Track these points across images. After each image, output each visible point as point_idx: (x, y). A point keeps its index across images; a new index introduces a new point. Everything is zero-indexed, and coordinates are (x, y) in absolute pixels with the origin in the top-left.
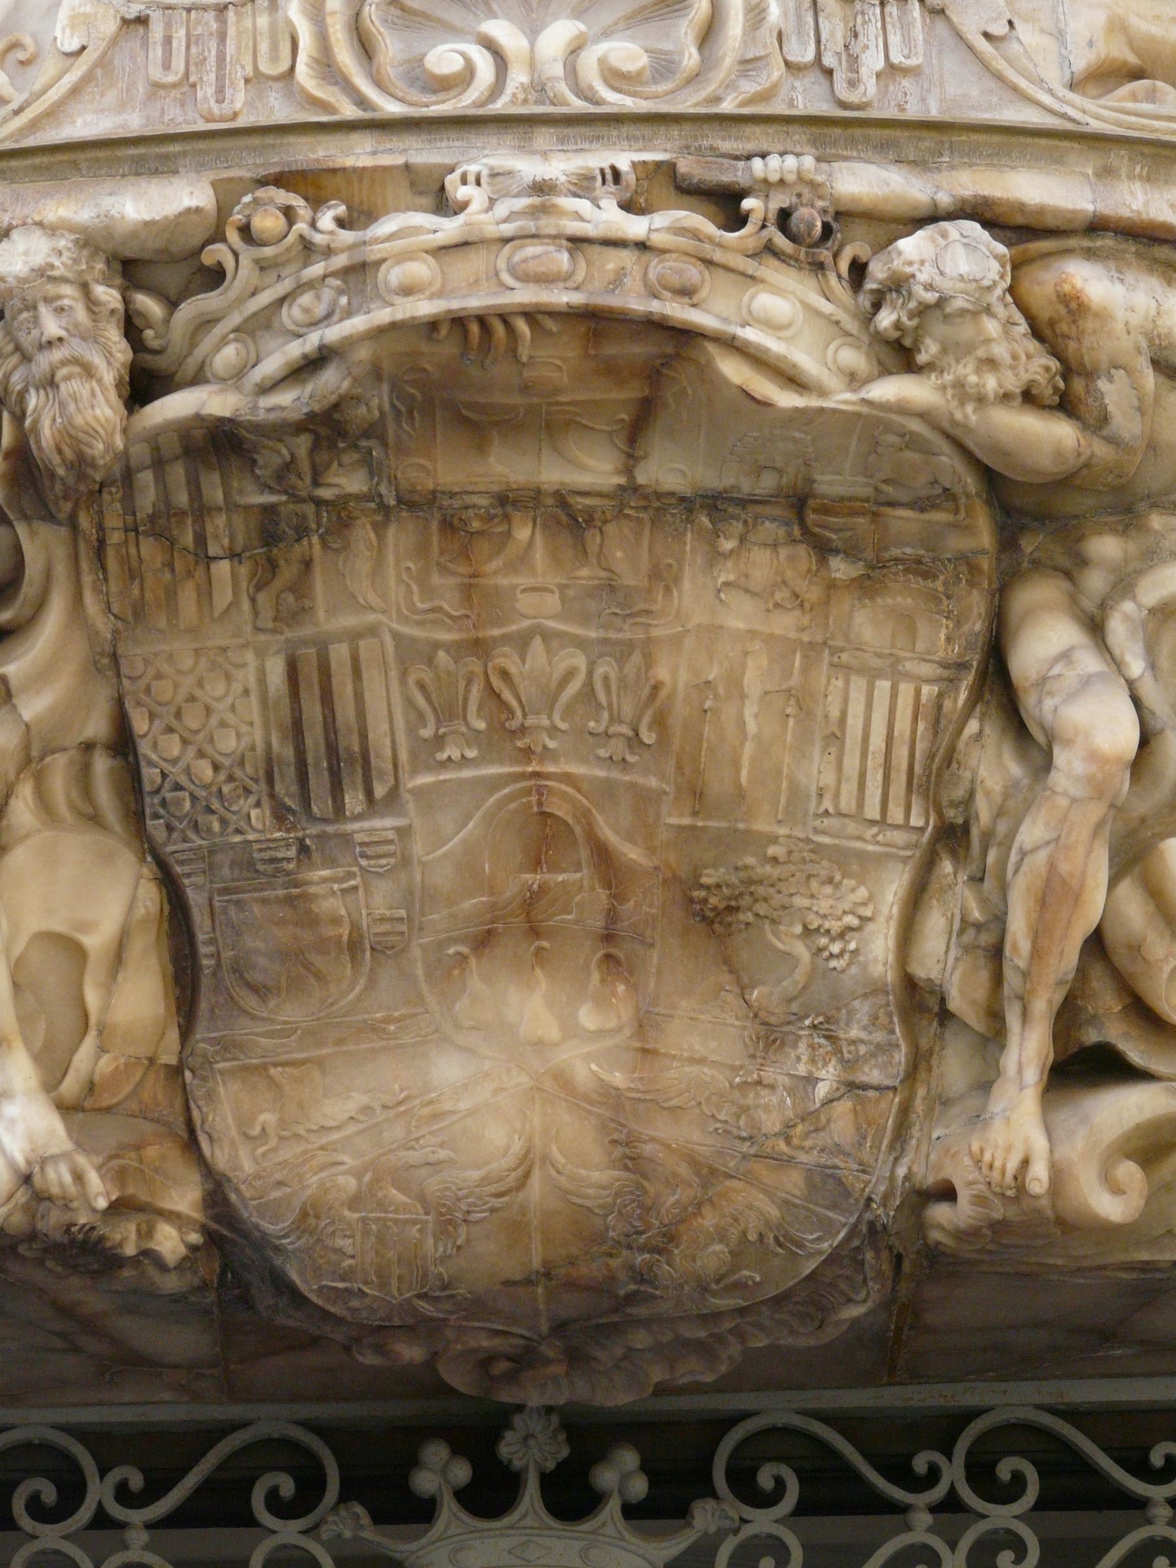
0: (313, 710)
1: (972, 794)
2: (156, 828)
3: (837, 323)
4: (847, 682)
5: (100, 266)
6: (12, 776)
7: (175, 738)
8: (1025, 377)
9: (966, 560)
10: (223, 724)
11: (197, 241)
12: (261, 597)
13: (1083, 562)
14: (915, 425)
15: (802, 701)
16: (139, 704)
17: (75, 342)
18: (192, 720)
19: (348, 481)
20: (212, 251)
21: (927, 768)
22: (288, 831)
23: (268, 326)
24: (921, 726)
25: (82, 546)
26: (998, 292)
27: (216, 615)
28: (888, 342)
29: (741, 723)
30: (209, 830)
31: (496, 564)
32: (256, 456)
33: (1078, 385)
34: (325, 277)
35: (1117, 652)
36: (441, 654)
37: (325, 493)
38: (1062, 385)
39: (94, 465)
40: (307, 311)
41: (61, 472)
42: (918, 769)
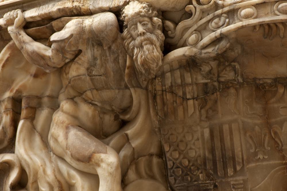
0: (218, 144)
2: (171, 180)
5: (155, 12)
6: (129, 163)
7: (177, 152)
10: (191, 149)
11: (184, 5)
12: (203, 111)
16: (166, 143)
17: (148, 34)
18: (182, 148)
19: (228, 75)
20: (188, 7)
22: (211, 180)
23: (205, 29)
25: (150, 95)
27: (189, 116)
30: (187, 180)
31: (273, 100)
32: (201, 68)
34: (222, 14)
36: (257, 127)
37: (222, 79)
39: (153, 70)
40: (216, 24)
41: (144, 72)
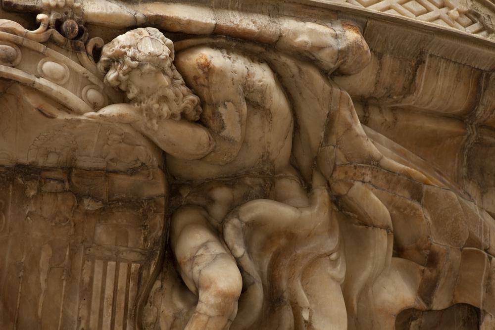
1: (157, 319)
3: (87, 77)
4: (93, 263)
8: (183, 105)
9: (151, 199)
13: (212, 201)
14: (127, 130)
15: (70, 273)
21: (135, 305)
24: (131, 284)
26: (169, 62)
28: (113, 88)
29: (38, 283)
33: (208, 111)
35: (230, 244)
38: (201, 109)
42: (130, 306)
